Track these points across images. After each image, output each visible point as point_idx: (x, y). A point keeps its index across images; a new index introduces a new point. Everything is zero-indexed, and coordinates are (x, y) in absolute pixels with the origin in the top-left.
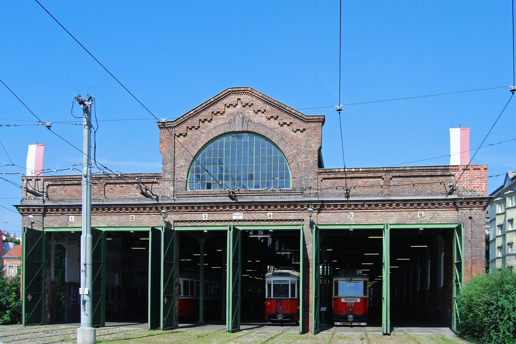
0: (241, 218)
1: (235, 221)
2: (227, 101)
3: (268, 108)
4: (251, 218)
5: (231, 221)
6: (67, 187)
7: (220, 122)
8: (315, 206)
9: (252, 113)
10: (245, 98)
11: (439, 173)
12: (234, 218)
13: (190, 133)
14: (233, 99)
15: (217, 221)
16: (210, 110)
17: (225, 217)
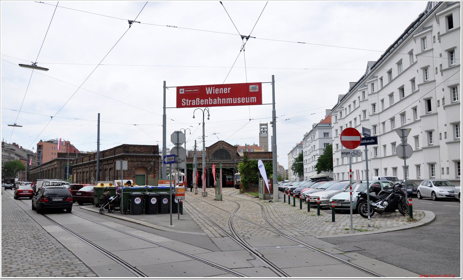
2: (219, 143)
3: (227, 145)
9: (224, 145)
10: (223, 143)
14: (220, 143)
16: (216, 145)
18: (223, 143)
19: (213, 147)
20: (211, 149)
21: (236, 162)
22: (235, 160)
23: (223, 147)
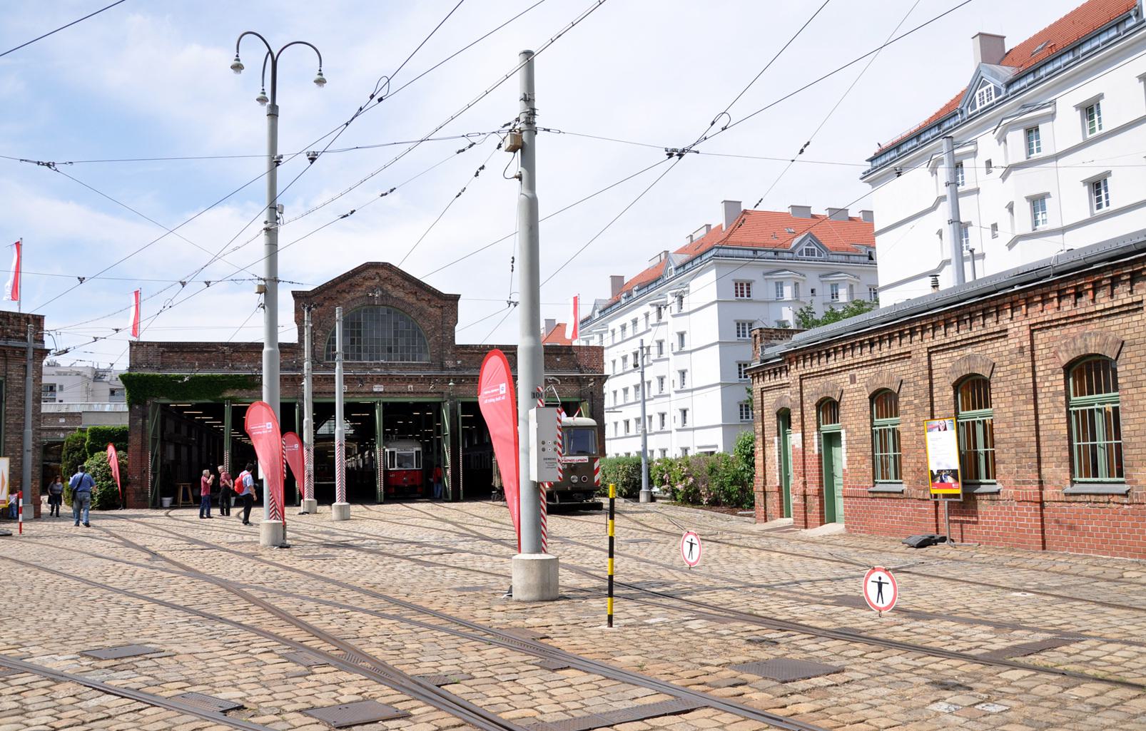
0: (382, 390)
1: (376, 392)
2: (363, 274)
4: (391, 390)
5: (371, 393)
6: (185, 355)
7: (358, 295)
8: (454, 380)
9: (390, 287)
10: (384, 273)
11: (564, 352)
12: (375, 390)
13: (326, 304)
14: (372, 272)
15: (357, 393)
16: (348, 282)
17: (366, 389)
18: (384, 273)
19: (333, 293)
20: (322, 305)
21: (454, 373)
22: (449, 363)
23: (386, 295)
